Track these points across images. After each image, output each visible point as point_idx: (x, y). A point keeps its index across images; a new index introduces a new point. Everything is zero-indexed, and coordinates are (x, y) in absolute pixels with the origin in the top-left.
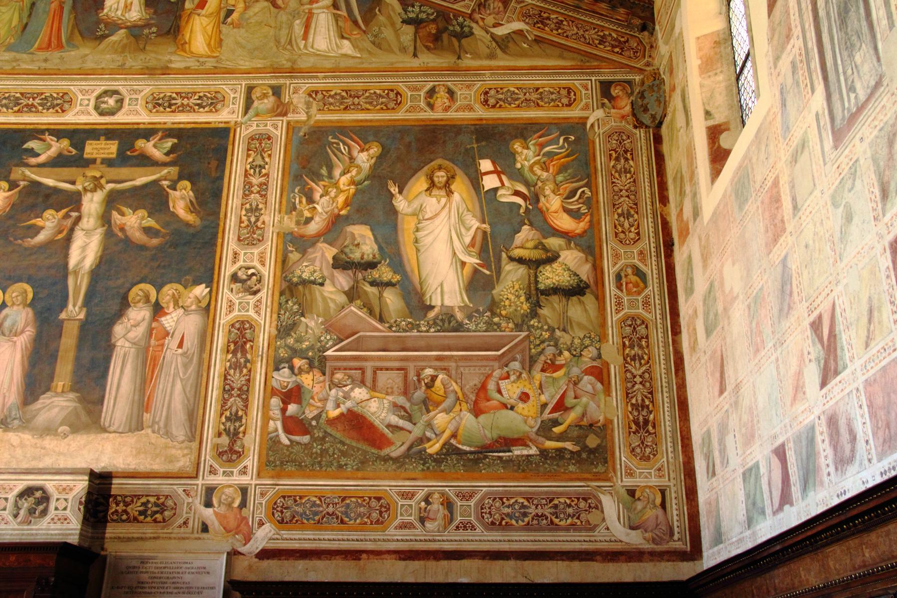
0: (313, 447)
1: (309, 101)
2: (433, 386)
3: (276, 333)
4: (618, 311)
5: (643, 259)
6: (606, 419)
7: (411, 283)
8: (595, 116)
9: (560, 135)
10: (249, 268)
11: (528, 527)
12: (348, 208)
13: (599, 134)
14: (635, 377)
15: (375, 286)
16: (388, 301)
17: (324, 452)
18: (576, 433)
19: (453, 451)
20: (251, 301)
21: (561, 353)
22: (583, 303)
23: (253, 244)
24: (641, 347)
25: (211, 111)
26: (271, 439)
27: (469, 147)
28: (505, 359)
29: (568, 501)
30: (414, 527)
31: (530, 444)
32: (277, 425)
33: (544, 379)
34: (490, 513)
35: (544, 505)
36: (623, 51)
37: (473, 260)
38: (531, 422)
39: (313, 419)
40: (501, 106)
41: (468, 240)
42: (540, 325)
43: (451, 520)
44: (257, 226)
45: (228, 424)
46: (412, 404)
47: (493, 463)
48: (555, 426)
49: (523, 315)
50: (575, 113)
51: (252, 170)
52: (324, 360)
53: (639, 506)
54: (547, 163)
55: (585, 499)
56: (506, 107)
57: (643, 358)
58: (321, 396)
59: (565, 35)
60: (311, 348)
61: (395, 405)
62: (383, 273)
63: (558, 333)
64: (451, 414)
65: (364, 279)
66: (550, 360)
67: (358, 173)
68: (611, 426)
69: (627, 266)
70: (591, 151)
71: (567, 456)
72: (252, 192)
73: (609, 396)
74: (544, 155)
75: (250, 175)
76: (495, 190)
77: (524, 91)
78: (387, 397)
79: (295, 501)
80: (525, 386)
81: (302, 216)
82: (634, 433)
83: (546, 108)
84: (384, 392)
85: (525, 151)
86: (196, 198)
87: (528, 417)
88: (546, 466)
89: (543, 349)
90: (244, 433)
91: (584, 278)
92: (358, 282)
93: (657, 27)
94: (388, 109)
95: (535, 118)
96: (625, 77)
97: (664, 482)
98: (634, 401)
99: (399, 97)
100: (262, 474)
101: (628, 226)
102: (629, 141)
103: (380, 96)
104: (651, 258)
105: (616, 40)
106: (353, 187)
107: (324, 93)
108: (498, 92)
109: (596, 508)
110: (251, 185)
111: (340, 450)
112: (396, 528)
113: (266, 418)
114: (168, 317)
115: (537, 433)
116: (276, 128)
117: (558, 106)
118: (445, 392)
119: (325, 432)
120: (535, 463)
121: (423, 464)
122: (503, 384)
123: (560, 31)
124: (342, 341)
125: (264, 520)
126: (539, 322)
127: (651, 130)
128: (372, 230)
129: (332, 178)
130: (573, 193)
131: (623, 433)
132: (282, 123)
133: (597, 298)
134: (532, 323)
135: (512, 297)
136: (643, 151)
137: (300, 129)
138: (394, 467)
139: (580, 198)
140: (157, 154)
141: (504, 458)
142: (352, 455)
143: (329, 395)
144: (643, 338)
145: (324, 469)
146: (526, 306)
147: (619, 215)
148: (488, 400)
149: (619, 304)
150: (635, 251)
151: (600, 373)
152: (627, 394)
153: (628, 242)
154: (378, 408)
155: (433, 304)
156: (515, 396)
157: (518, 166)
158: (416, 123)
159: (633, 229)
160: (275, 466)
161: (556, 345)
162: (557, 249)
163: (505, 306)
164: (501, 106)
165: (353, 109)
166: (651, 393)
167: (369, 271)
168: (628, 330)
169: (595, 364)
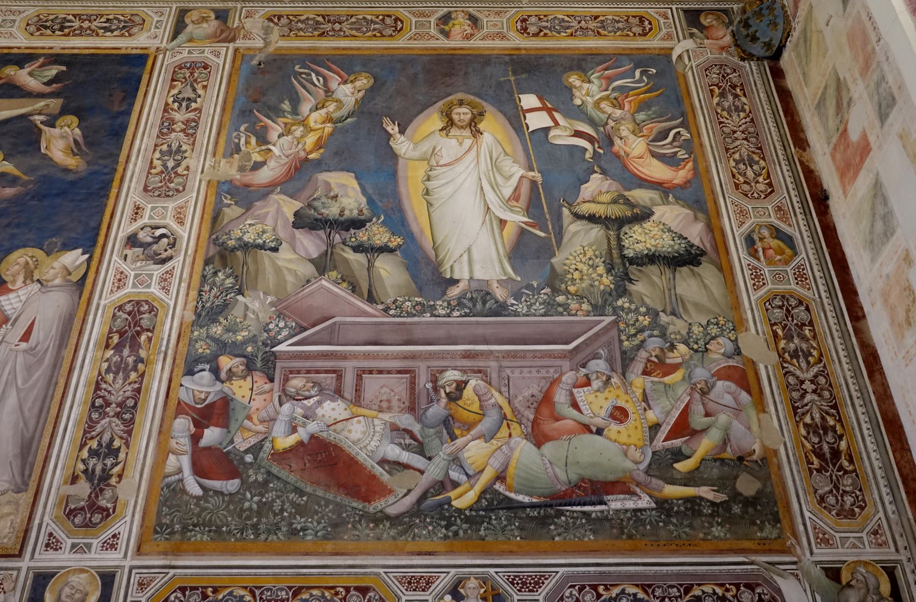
0: (244, 499)
1: (268, 26)
2: (460, 398)
3: (194, 318)
4: (757, 288)
5: (784, 218)
6: (765, 448)
7: (420, 248)
8: (682, 46)
10: (158, 228)
12: (322, 151)
13: (692, 67)
14: (802, 382)
15: (361, 252)
16: (383, 272)
17: (264, 508)
18: (715, 471)
19: (499, 503)
20: (156, 273)
21: (672, 347)
22: (699, 275)
23: (168, 196)
24: (803, 338)
25: (123, 35)
26: (168, 486)
27: (502, 79)
28: (580, 357)
29: (719, 591)
31: (638, 490)
33: (648, 386)
35: (676, 597)
37: (517, 218)
38: (637, 455)
39: (247, 451)
40: (545, 35)
41: (508, 192)
42: (633, 307)
44: (176, 173)
45: (92, 462)
46: (425, 426)
47: (574, 523)
49: (603, 293)
50: (654, 43)
51: (176, 104)
52: (272, 358)
54: (619, 99)
55: (750, 587)
56: (553, 36)
57: (811, 355)
58: (264, 414)
60: (253, 340)
61: (395, 428)
62: (374, 235)
63: (664, 318)
64: (494, 441)
65: (344, 243)
66: (656, 356)
67: (339, 108)
68: (775, 460)
69: (761, 226)
70: (683, 86)
71: (707, 511)
72: (174, 130)
73: (764, 412)
74: (613, 89)
75: (172, 109)
76: (547, 130)
77: (577, 18)
78: (381, 415)
80: (618, 396)
81: (250, 160)
82: (818, 471)
83: (611, 38)
84: (376, 407)
85: (586, 86)
86: (85, 137)
87: (629, 445)
88: (671, 527)
90: (120, 476)
91: (696, 242)
92: (333, 247)
94: (383, 36)
95: (596, 48)
96: (718, 6)
97: (888, 554)
98: (808, 419)
99: (399, 23)
100: (145, 548)
101: (753, 175)
102: (735, 74)
103: (372, 21)
104: (795, 215)
106: (329, 125)
107: (291, 17)
108: (540, 19)
110: (173, 122)
111: (293, 504)
113: (163, 451)
114: (11, 295)
115: (647, 472)
116: (218, 55)
117: (628, 35)
118: (481, 407)
119: (269, 473)
120: (651, 523)
121: (447, 527)
122: (581, 395)
124: (305, 329)
126: (631, 302)
127: (766, 63)
128: (357, 178)
129: (297, 114)
130: (663, 135)
131: (799, 472)
132: (227, 51)
133: (721, 269)
134: (620, 303)
135: (585, 268)
136: (759, 86)
137: (252, 57)
138: (393, 532)
139: (674, 140)
140: (33, 84)
141: (594, 515)
142: (316, 512)
143: (278, 413)
144: (804, 325)
145: (263, 537)
146: (607, 280)
147: (737, 162)
148: (557, 419)
149: (757, 276)
150: (770, 207)
152: (795, 409)
153: (756, 195)
154: (364, 433)
155: (456, 277)
156: (603, 413)
157: (578, 102)
158: (424, 52)
159: (761, 179)
160: (172, 533)
161: (663, 335)
162: (648, 203)
163: (573, 280)
165: (333, 36)
166: (835, 407)
167: (352, 231)
168: (778, 314)
169: (731, 363)
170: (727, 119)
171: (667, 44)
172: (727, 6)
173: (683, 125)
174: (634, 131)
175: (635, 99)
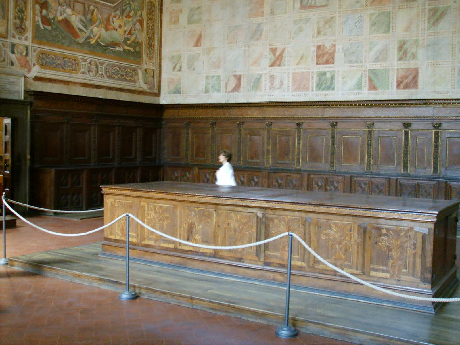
11: (119, 79)
21: (131, 11)
26: (37, 25)
29: (130, 71)
30: (86, 74)
31: (121, 46)
32: (38, 18)
34: (109, 71)
38: (122, 37)
43: (97, 72)
48: (128, 41)
53: (147, 75)
55: (134, 71)
64: (99, 28)
78: (78, 15)
79: (47, 56)
89: (126, 8)
109: (137, 74)
112: (81, 73)
113: (34, 14)
115: (123, 42)
118: (97, 18)
119: (57, 26)
125: (36, 63)
138: (80, 47)
143: (58, 9)
151: (141, 22)
156: (118, 26)
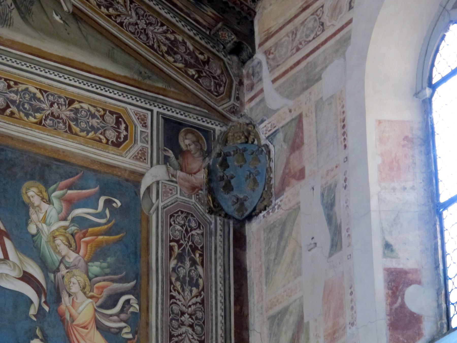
9: (102, 193)
13: (157, 208)
36: (200, 77)
40: (12, 113)
54: (77, 236)
56: (21, 119)
59: (119, 20)
74: (73, 220)
77: (51, 98)
83: (82, 139)
85: (45, 206)
93: (259, 56)
95: (64, 151)
96: (200, 122)
105: (191, 54)
108: (9, 87)
117: (100, 141)
123: (111, 10)
127: (231, 222)
136: (219, 255)
139: (122, 310)
164: (12, 113)
170: (179, 293)
171: (138, 166)
172: (209, 125)
173: (134, 291)
174: (84, 288)
175: (93, 240)
